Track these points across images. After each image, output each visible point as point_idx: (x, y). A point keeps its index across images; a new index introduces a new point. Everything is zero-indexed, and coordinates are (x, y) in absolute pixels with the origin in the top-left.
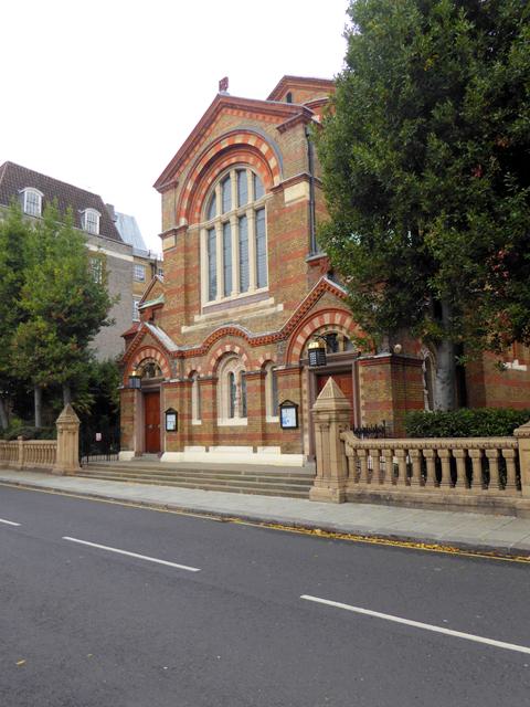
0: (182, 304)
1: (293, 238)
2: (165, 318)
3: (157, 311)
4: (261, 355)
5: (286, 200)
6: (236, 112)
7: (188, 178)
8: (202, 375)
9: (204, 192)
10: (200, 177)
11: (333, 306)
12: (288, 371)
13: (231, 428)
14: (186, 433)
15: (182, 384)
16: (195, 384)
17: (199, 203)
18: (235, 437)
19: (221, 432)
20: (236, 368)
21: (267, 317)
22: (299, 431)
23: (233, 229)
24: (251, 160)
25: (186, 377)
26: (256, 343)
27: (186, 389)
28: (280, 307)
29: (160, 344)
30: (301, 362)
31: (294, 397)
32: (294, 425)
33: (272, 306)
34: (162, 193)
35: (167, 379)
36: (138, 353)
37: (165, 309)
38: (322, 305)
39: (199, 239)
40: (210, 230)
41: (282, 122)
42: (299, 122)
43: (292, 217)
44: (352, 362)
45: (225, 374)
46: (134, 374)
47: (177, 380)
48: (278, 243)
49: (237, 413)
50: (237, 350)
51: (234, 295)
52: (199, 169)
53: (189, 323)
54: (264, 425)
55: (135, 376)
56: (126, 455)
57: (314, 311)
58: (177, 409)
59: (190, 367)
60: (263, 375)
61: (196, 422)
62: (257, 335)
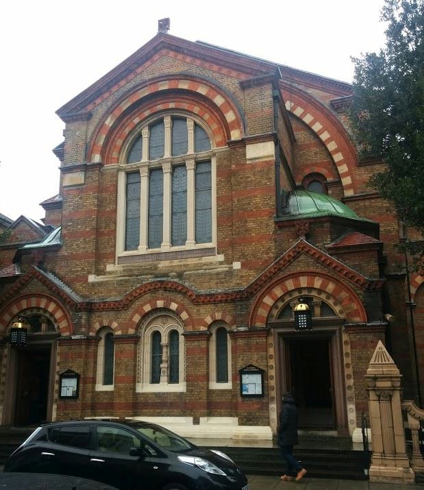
0: (90, 248)
1: (255, 196)
3: (50, 255)
4: (208, 316)
5: (248, 156)
6: (180, 57)
7: (109, 112)
11: (312, 269)
13: (157, 395)
21: (218, 274)
24: (196, 109)
26: (199, 300)
27: (92, 348)
28: (237, 265)
30: (267, 324)
31: (255, 359)
32: (261, 393)
35: (66, 334)
36: (18, 300)
37: (64, 252)
38: (297, 267)
40: (133, 174)
41: (243, 78)
42: (269, 82)
43: (254, 175)
48: (235, 200)
50: (174, 306)
51: (166, 247)
52: (125, 106)
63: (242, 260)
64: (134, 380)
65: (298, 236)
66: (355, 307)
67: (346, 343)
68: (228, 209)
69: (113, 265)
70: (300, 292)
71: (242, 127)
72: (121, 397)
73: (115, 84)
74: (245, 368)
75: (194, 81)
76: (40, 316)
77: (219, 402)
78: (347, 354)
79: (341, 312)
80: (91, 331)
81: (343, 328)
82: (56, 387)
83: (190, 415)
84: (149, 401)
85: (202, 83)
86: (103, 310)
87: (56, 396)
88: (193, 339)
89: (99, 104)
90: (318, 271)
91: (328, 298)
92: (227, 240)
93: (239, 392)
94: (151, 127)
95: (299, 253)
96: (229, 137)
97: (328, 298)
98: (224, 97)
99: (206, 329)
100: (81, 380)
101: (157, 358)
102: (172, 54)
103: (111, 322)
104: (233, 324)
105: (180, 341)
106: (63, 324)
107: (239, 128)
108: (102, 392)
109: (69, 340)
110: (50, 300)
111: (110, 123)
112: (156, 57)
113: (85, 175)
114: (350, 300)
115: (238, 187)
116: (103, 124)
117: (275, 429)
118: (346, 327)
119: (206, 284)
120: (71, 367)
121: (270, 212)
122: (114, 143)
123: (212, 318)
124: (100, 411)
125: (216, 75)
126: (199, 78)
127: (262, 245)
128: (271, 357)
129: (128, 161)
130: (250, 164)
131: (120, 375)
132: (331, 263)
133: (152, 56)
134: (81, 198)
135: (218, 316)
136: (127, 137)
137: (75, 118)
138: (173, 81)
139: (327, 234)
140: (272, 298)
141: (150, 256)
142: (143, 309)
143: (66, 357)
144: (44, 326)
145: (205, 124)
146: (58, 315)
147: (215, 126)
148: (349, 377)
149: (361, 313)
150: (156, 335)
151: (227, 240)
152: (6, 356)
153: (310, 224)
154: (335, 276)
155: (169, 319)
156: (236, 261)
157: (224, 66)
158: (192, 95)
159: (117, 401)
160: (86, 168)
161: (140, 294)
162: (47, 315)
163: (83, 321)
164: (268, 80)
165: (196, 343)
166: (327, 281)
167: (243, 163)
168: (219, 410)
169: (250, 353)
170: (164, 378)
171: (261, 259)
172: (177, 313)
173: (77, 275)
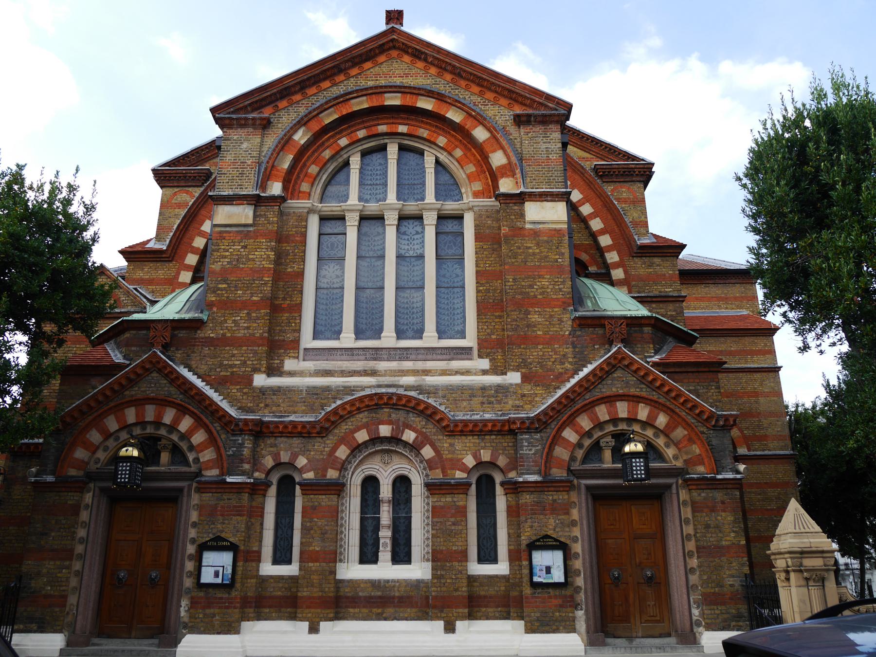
0: (259, 330)
1: (540, 276)
3: (182, 334)
6: (420, 64)
10: (326, 129)
11: (633, 391)
12: (547, 484)
13: (375, 584)
22: (568, 592)
24: (442, 141)
30: (570, 471)
31: (551, 525)
32: (562, 580)
33: (485, 372)
35: (212, 473)
37: (209, 333)
38: (607, 389)
41: (518, 110)
50: (409, 436)
52: (328, 118)
53: (272, 371)
57: (597, 394)
62: (460, 416)
63: (523, 370)
64: (334, 557)
65: (611, 343)
66: (698, 451)
67: (685, 503)
68: (495, 290)
69: (296, 361)
70: (615, 425)
71: (519, 175)
72: (312, 586)
73: (313, 84)
74: (538, 540)
75: (441, 100)
76: (158, 439)
77: (485, 597)
78: (687, 522)
79: (676, 457)
80: (257, 470)
81: (680, 481)
82: (190, 566)
83: (438, 618)
84: (361, 594)
85: (454, 106)
86: (282, 434)
87: (188, 583)
88: (441, 492)
89: (284, 109)
90: (644, 394)
91: (656, 435)
92: (494, 337)
93: (526, 579)
94: (364, 154)
95: (614, 366)
96: (496, 186)
97: (656, 435)
98: (489, 130)
99: (465, 475)
100: (241, 556)
101: (370, 521)
102: (407, 58)
103: (295, 456)
104: (511, 470)
105: (413, 493)
106: (208, 455)
107: (513, 175)
108: (271, 577)
109: (220, 485)
110: (183, 411)
111: (301, 138)
112: (382, 58)
113: (255, 212)
114: (691, 441)
115: (513, 260)
116: (290, 138)
117: (585, 638)
118: (686, 481)
119: (465, 403)
120: (222, 531)
121: (564, 303)
122: (305, 170)
123: (475, 456)
124: (267, 610)
125: (476, 99)
126: (450, 98)
127: (553, 350)
128: (573, 523)
129: (321, 200)
130: (531, 229)
131: (311, 548)
132: (662, 385)
133: (376, 55)
134: (245, 247)
135: (486, 456)
136: (325, 164)
137: (243, 122)
138: (409, 95)
139: (649, 343)
140: (577, 432)
141: (361, 352)
142: (354, 438)
143: (209, 513)
144: (165, 457)
145: (456, 163)
146: (199, 438)
147: (471, 168)
148: (691, 554)
149: (706, 460)
150: (370, 484)
151: (494, 337)
152: (87, 506)
153: (627, 325)
154: (668, 403)
155: (396, 459)
156: (513, 370)
157: (490, 89)
158: (436, 119)
159: (304, 593)
160: (257, 201)
161: (349, 412)
162: (175, 437)
163: (246, 452)
164: (556, 119)
165: (449, 499)
166: (656, 411)
167: (521, 226)
168: (484, 609)
169: (542, 517)
170: (385, 555)
171: (552, 370)
172: (415, 448)
173: (232, 373)
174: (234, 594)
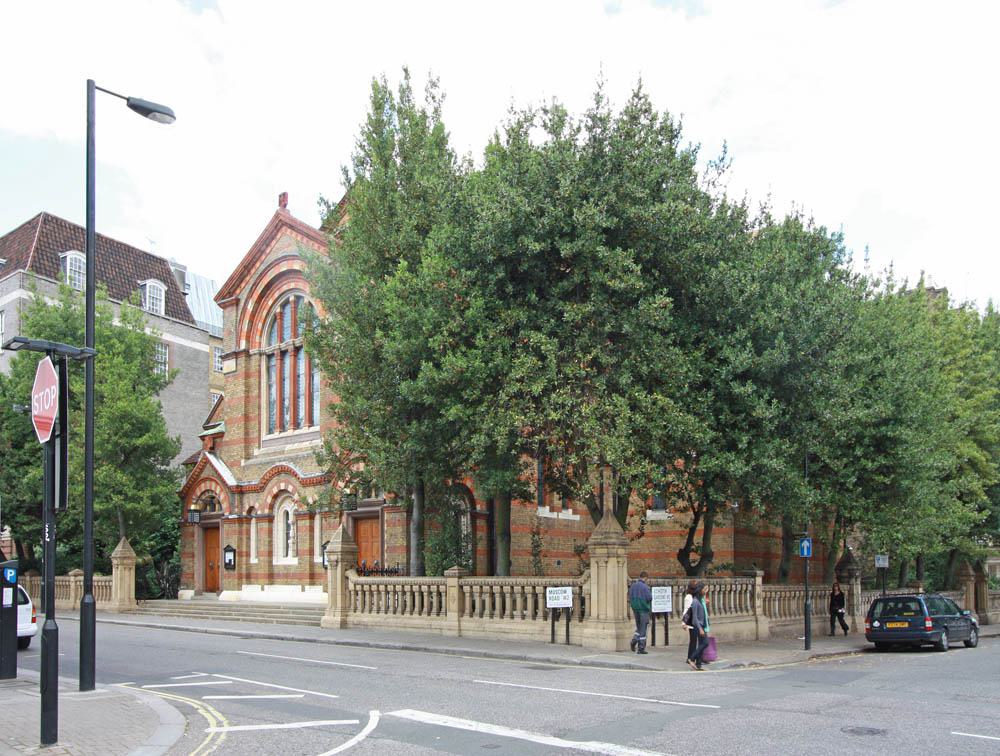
0: (242, 435)
2: (226, 448)
3: (218, 440)
8: (259, 512)
9: (264, 314)
13: (286, 567)
14: (244, 571)
15: (240, 520)
16: (253, 521)
17: (260, 325)
18: (288, 577)
19: (276, 571)
20: (290, 507)
23: (288, 361)
25: (244, 514)
27: (245, 526)
29: (219, 476)
34: (223, 308)
39: (260, 366)
44: (378, 508)
45: (281, 513)
46: (193, 507)
47: (236, 516)
49: (290, 552)
50: (290, 488)
54: (312, 565)
55: (195, 511)
56: (186, 594)
58: (234, 546)
59: (249, 502)
60: (312, 516)
61: (254, 560)
136: (265, 320)
174: (236, 572)
